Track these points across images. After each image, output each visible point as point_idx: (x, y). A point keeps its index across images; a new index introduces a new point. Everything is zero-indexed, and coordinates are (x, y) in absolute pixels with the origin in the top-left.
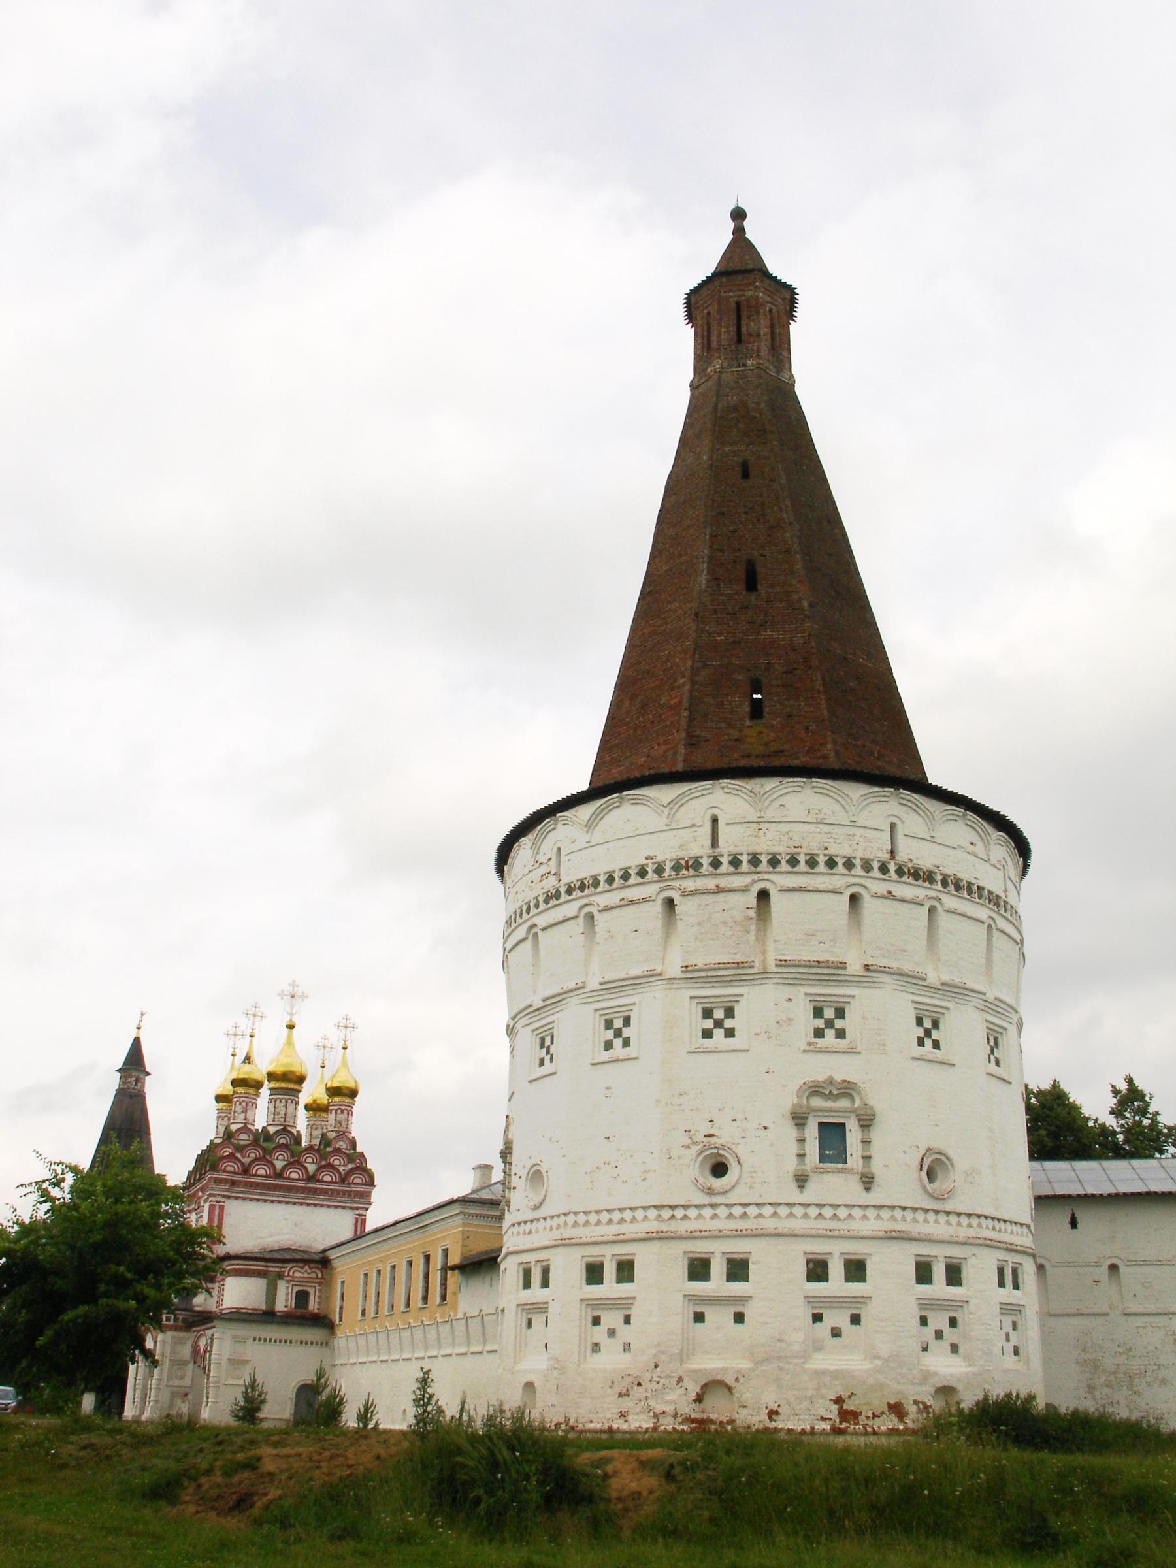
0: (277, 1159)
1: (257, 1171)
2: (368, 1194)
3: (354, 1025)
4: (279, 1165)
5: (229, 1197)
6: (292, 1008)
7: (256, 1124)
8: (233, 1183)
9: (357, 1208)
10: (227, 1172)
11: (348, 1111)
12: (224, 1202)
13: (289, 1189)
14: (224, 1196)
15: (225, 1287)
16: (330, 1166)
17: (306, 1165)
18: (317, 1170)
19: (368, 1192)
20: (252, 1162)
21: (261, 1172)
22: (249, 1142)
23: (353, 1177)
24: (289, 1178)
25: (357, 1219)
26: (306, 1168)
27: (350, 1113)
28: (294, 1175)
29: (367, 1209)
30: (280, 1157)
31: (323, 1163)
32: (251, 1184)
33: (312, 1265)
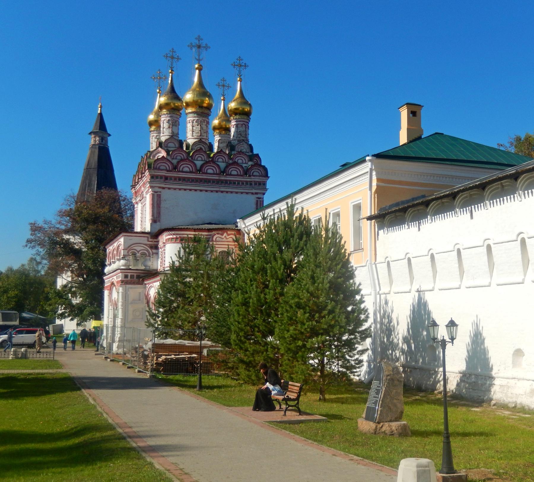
0: (197, 160)
1: (183, 169)
2: (265, 184)
3: (245, 64)
4: (199, 163)
5: (164, 188)
6: (199, 56)
7: (179, 136)
8: (166, 178)
9: (256, 193)
10: (162, 170)
11: (246, 126)
12: (160, 192)
13: (207, 181)
14: (160, 187)
15: (166, 251)
16: (235, 163)
17: (218, 163)
18: (227, 167)
19: (264, 182)
20: (178, 163)
21: (186, 169)
22: (175, 149)
23: (252, 172)
24: (207, 173)
25: (257, 201)
26: (218, 166)
27: (247, 126)
28: (210, 171)
29: (264, 194)
30: (199, 159)
31: (231, 162)
32: (180, 179)
33: (229, 232)
